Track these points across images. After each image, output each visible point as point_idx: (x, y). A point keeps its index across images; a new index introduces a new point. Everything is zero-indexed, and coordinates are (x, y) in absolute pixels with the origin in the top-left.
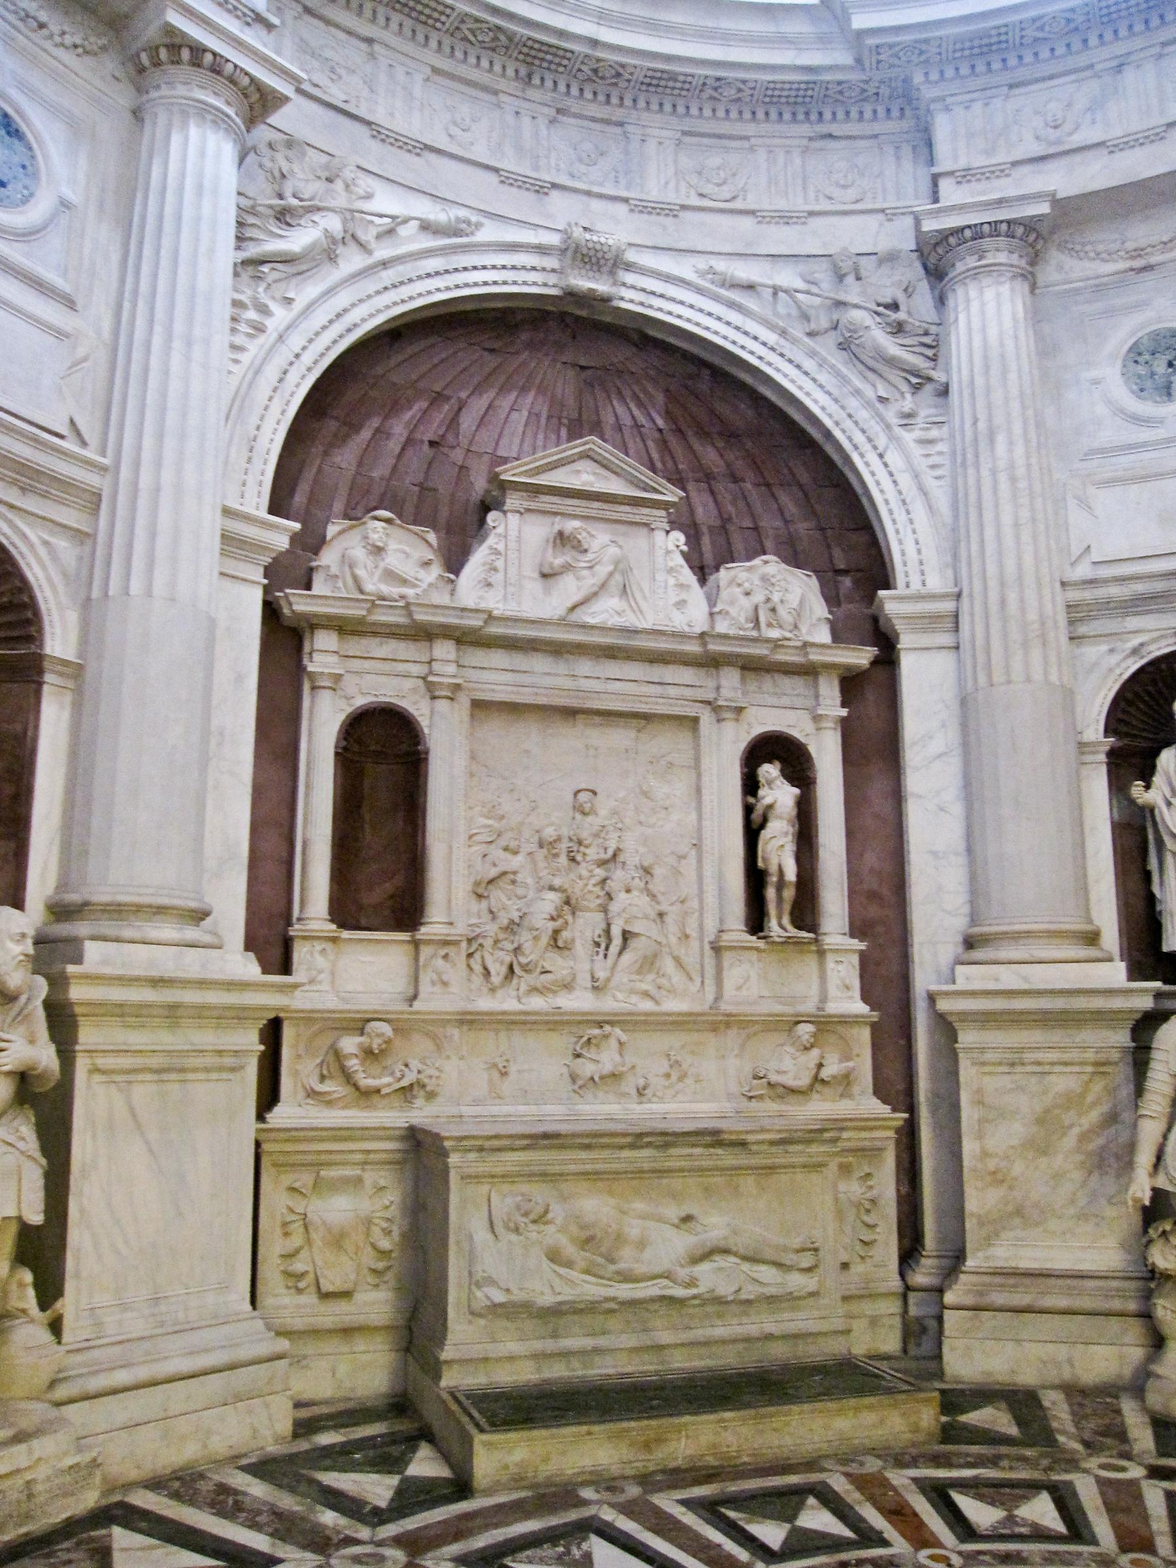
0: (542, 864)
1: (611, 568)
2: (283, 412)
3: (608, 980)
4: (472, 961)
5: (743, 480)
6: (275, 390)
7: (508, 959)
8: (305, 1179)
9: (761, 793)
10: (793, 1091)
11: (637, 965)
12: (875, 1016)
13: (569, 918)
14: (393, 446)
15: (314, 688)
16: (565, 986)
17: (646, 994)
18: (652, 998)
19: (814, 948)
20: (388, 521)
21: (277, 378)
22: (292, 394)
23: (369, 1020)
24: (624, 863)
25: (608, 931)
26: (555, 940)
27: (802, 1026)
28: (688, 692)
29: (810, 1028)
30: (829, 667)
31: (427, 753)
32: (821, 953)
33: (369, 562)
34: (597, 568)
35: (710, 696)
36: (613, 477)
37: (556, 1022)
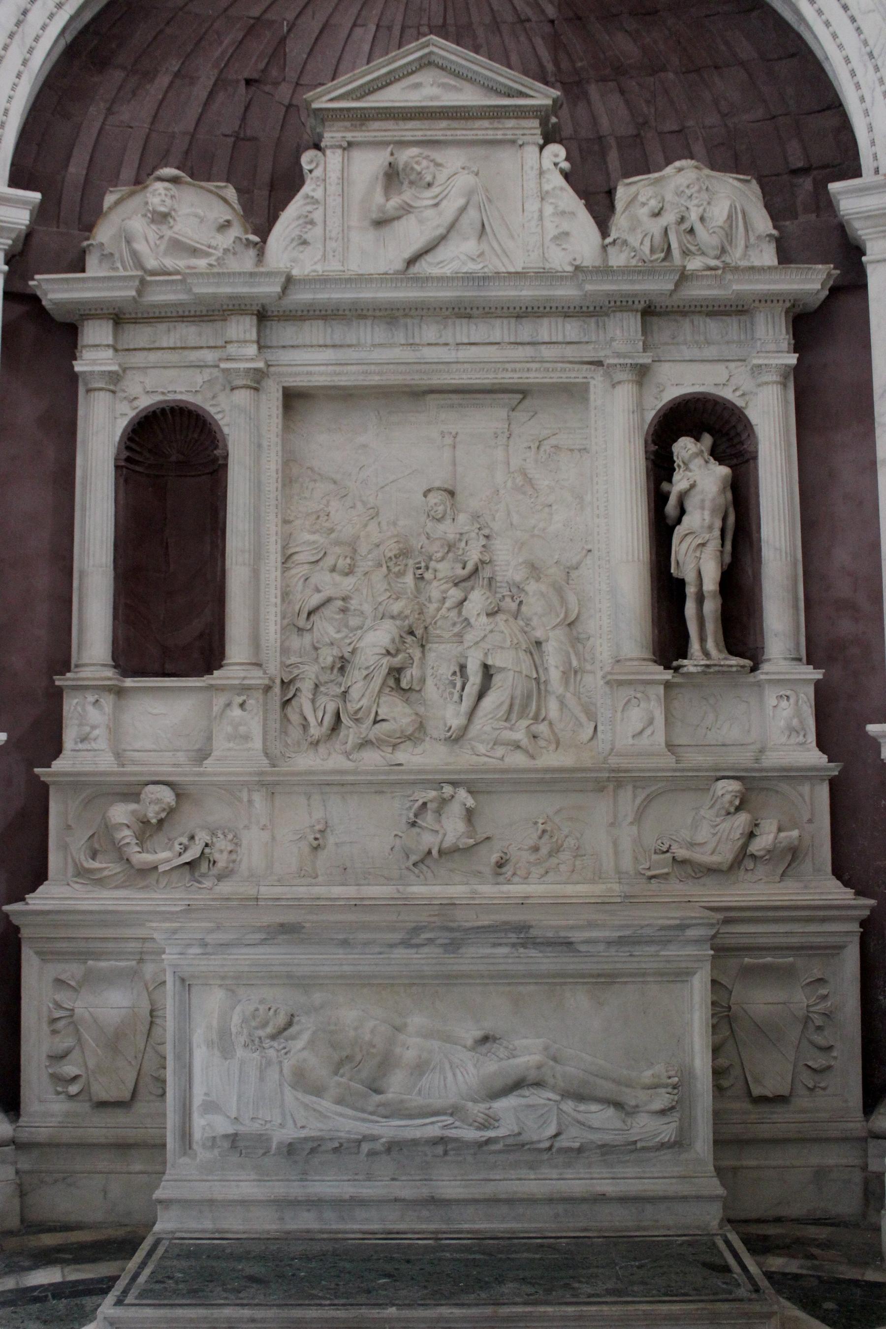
0: (381, 586)
1: (461, 202)
2: (25, 63)
3: (466, 728)
4: (289, 710)
5: (663, 69)
6: (11, 36)
7: (331, 707)
8: (72, 970)
9: (676, 477)
10: (711, 871)
11: (505, 707)
12: (834, 769)
13: (417, 653)
14: (200, 92)
15: (88, 391)
16: (409, 738)
17: (518, 746)
18: (526, 752)
19: (751, 678)
20: (174, 180)
21: (14, 21)
22: (37, 39)
23: (147, 784)
24: (491, 579)
25: (463, 667)
26: (398, 681)
27: (721, 783)
28: (570, 352)
29: (734, 786)
30: (767, 300)
31: (226, 457)
32: (759, 685)
33: (152, 231)
34: (444, 203)
35: (600, 355)
36: (466, 85)
37: (382, 783)
